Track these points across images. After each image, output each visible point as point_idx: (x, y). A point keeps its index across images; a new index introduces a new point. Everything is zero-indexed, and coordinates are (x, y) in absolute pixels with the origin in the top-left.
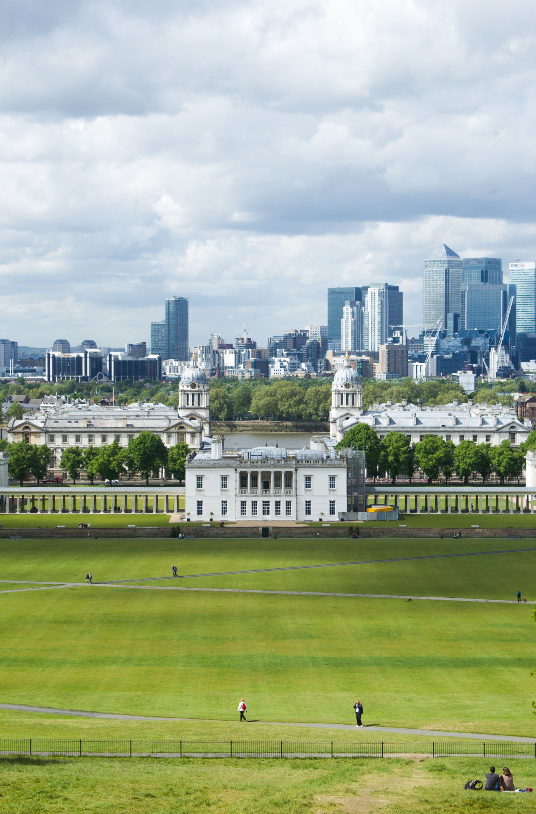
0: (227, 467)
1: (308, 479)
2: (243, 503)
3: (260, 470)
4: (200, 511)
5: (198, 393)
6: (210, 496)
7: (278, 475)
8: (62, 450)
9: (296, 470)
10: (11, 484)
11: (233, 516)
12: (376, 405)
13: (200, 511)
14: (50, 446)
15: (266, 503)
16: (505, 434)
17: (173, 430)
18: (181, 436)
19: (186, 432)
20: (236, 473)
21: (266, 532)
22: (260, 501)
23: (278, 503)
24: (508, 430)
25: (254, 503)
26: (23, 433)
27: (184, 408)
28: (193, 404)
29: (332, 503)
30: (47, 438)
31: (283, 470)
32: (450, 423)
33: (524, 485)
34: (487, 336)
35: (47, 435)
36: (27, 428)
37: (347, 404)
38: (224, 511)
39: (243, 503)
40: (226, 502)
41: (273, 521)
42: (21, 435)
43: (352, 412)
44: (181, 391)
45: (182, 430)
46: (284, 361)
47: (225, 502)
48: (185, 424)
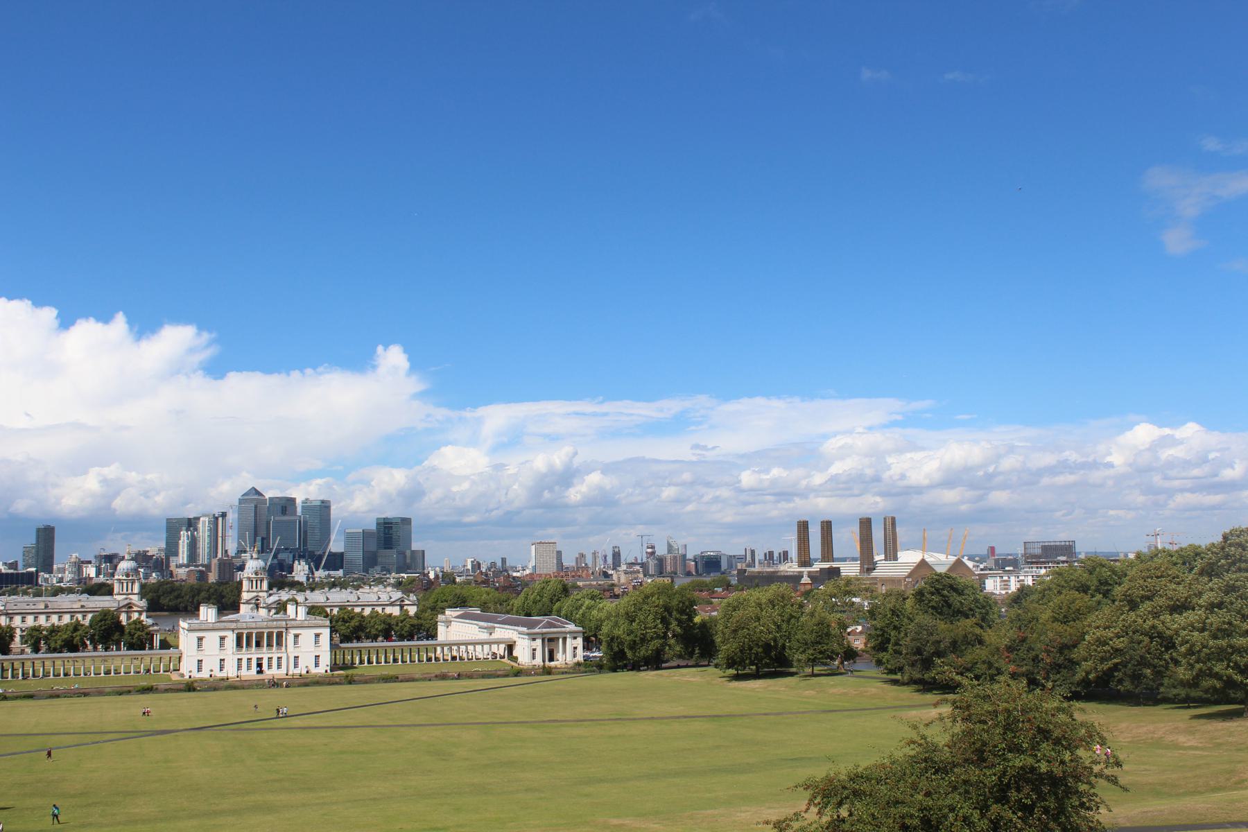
1: (296, 636)
2: (240, 660)
4: (199, 669)
7: (270, 635)
11: (230, 671)
12: (275, 590)
13: (199, 669)
23: (270, 659)
25: (249, 660)
29: (317, 657)
32: (353, 598)
39: (240, 660)
47: (222, 660)
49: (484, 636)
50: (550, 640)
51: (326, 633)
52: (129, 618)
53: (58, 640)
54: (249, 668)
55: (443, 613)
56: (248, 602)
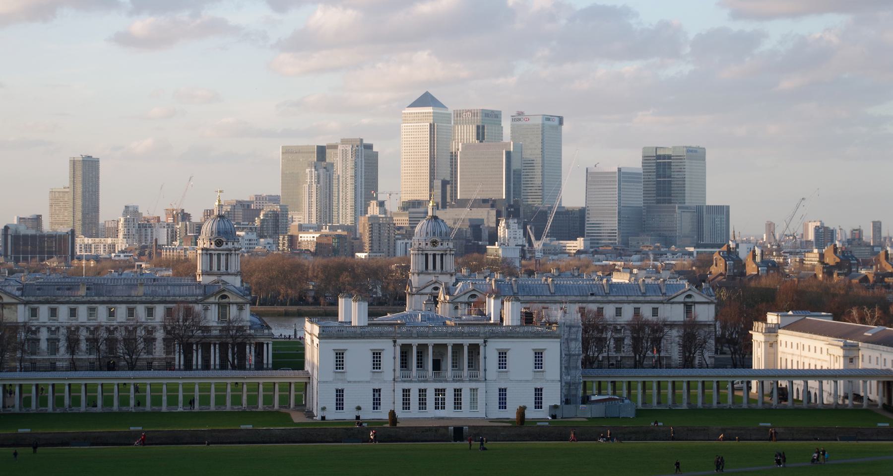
0: (380, 336)
1: (503, 356)
2: (406, 392)
3: (431, 342)
4: (340, 405)
5: (225, 252)
6: (355, 382)
8: (49, 329)
9: (485, 342)
13: (340, 405)
15: (439, 392)
16: (677, 305)
17: (212, 300)
18: (223, 308)
19: (229, 303)
20: (395, 346)
21: (459, 433)
22: (431, 388)
24: (682, 300)
25: (422, 392)
27: (204, 273)
28: (219, 270)
29: (538, 392)
30: (27, 313)
31: (466, 342)
34: (492, 206)
35: (27, 307)
38: (377, 403)
39: (406, 392)
40: (380, 390)
41: (451, 418)
43: (444, 279)
44: (202, 250)
45: (224, 300)
48: (230, 291)
49: (839, 365)
51: (552, 350)
52: (223, 315)
54: (422, 404)
55: (764, 320)
56: (419, 292)
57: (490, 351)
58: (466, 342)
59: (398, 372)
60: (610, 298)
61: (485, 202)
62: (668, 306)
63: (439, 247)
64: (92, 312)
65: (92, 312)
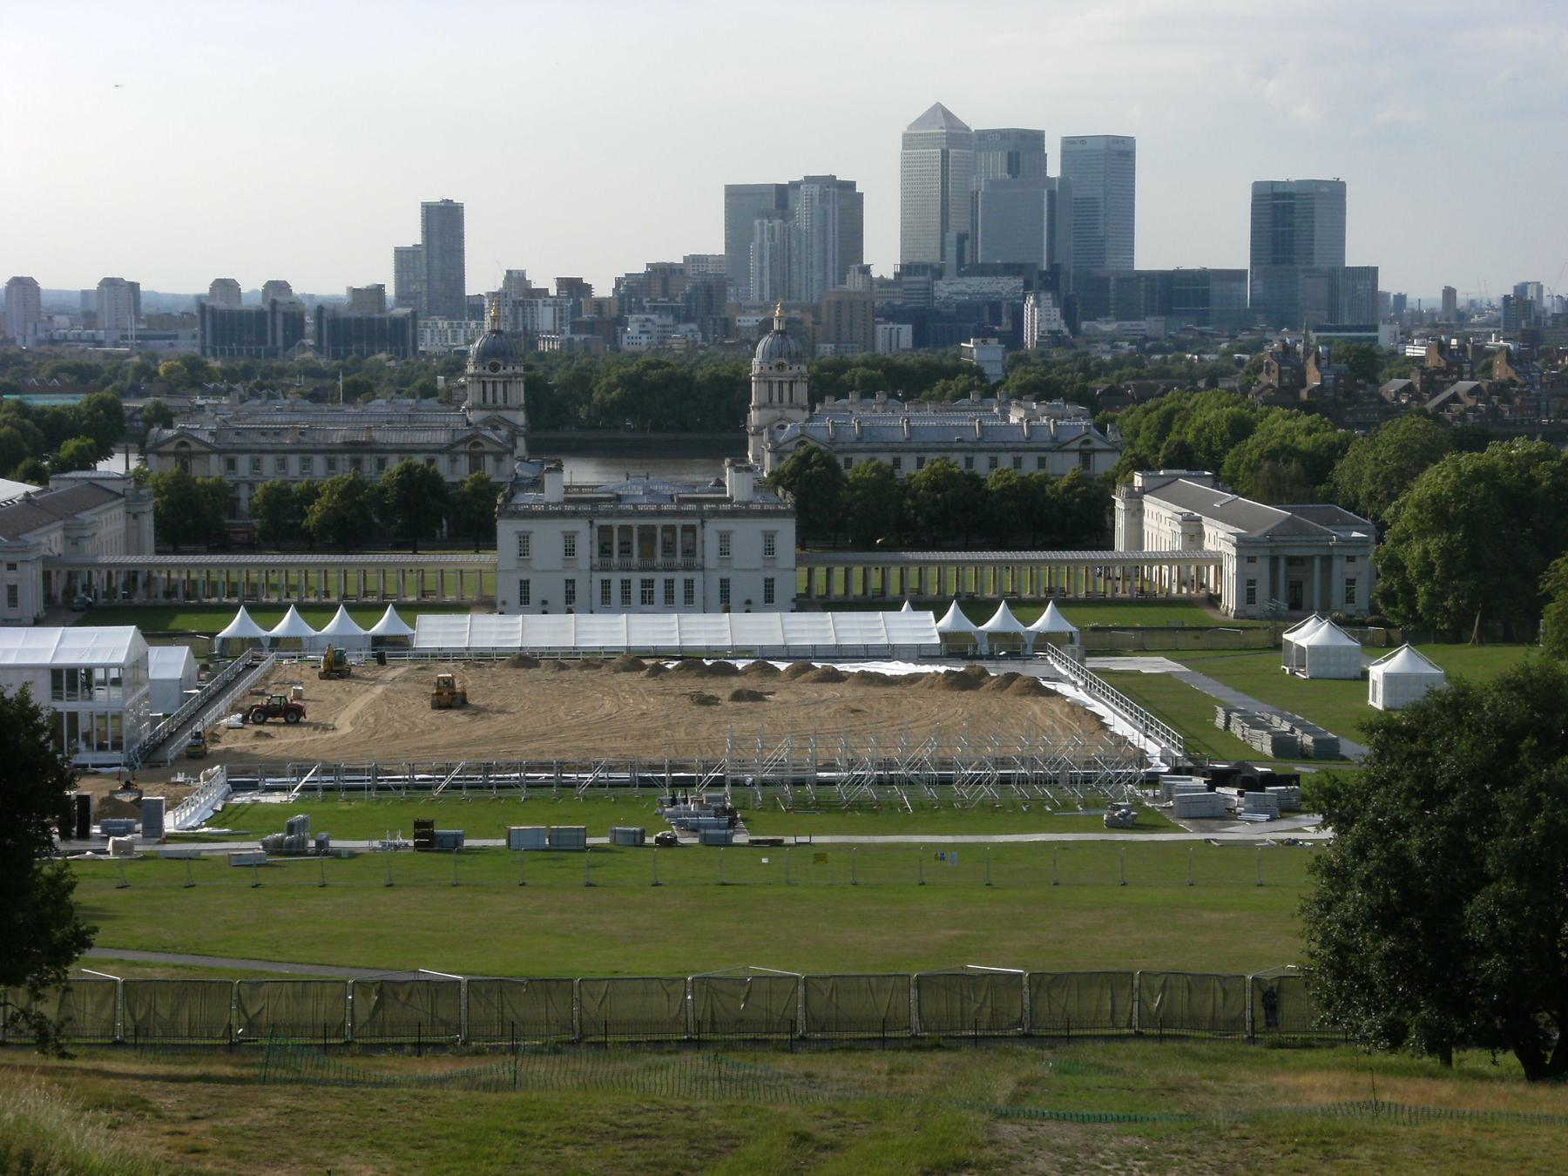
0: (575, 515)
1: (725, 537)
2: (606, 584)
10: (158, 553)
12: (829, 400)
14: (229, 479)
17: (461, 448)
18: (476, 463)
19: (484, 453)
23: (669, 584)
25: (626, 585)
26: (175, 454)
33: (1111, 547)
36: (184, 444)
37: (781, 400)
39: (606, 584)
42: (172, 459)
43: (790, 413)
46: (648, 320)
47: (573, 581)
50: (1291, 561)
51: (787, 531)
53: (315, 513)
57: (711, 531)
58: (679, 522)
59: (596, 560)
60: (982, 445)
61: (1011, 269)
62: (1059, 456)
63: (787, 371)
64: (306, 464)
65: (306, 464)
